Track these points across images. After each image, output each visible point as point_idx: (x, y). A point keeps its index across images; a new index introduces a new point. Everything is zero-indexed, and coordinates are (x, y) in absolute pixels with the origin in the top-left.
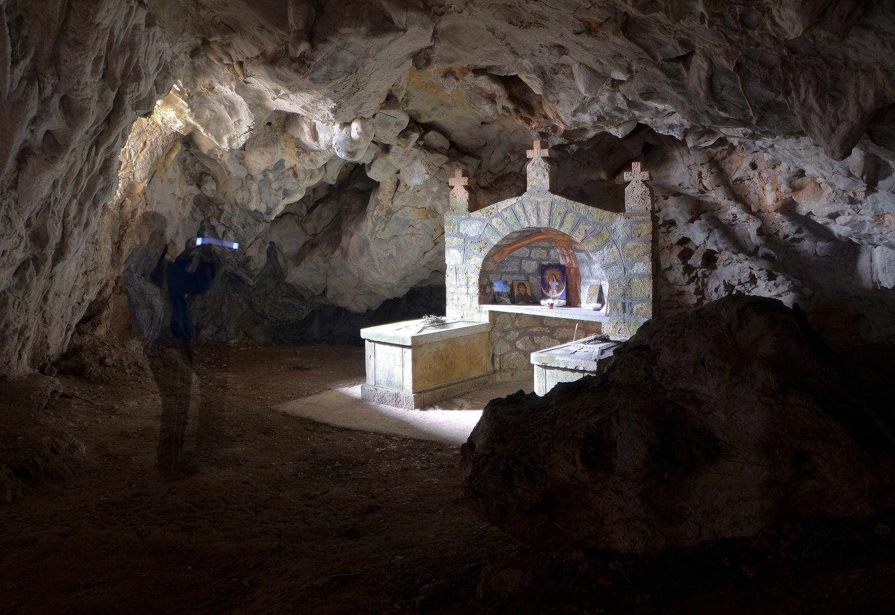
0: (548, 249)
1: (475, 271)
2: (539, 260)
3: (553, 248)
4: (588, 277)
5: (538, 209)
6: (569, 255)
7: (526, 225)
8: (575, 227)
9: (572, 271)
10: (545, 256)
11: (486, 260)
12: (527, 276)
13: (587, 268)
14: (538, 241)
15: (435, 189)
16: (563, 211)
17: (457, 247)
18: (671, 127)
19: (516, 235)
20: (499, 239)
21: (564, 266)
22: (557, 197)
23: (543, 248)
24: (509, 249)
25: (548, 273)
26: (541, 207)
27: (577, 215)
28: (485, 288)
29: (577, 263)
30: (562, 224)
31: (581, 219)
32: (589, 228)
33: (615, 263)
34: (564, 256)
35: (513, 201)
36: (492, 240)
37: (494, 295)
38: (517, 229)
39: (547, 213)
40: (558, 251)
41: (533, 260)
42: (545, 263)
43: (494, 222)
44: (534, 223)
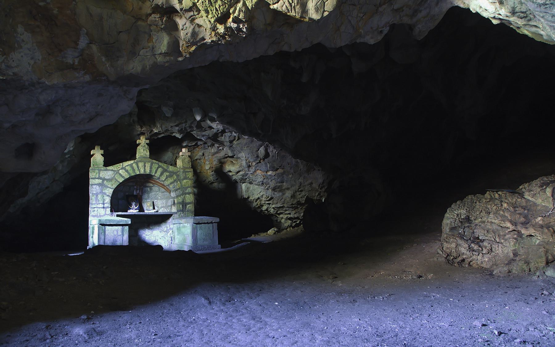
1: (108, 196)
5: (145, 166)
7: (138, 173)
8: (162, 174)
15: (67, 156)
16: (157, 166)
17: (99, 184)
18: (203, 136)
20: (123, 180)
22: (154, 161)
26: (146, 165)
27: (163, 168)
30: (156, 172)
31: (165, 171)
32: (168, 174)
33: (179, 189)
35: (132, 162)
36: (119, 180)
38: (133, 174)
39: (149, 168)
43: (120, 171)
44: (142, 172)
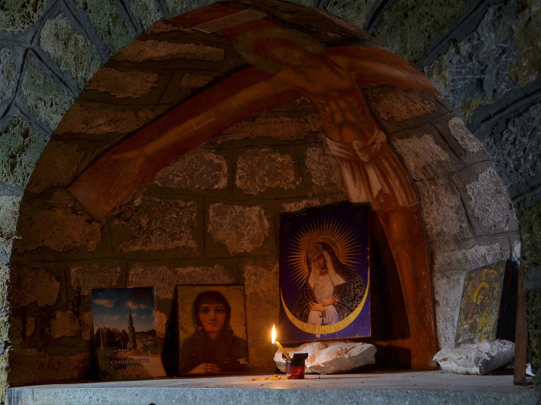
0: (295, 148)
2: (269, 199)
3: (315, 139)
4: (460, 241)
6: (375, 160)
9: (396, 228)
10: (289, 179)
11: (35, 201)
12: (235, 265)
13: (450, 201)
14: (250, 113)
19: (139, 85)
21: (365, 208)
23: (278, 145)
24: (135, 158)
25: (307, 241)
28: (46, 315)
29: (412, 187)
34: (359, 168)
37: (94, 344)
40: (334, 148)
41: (248, 201)
42: (291, 207)
